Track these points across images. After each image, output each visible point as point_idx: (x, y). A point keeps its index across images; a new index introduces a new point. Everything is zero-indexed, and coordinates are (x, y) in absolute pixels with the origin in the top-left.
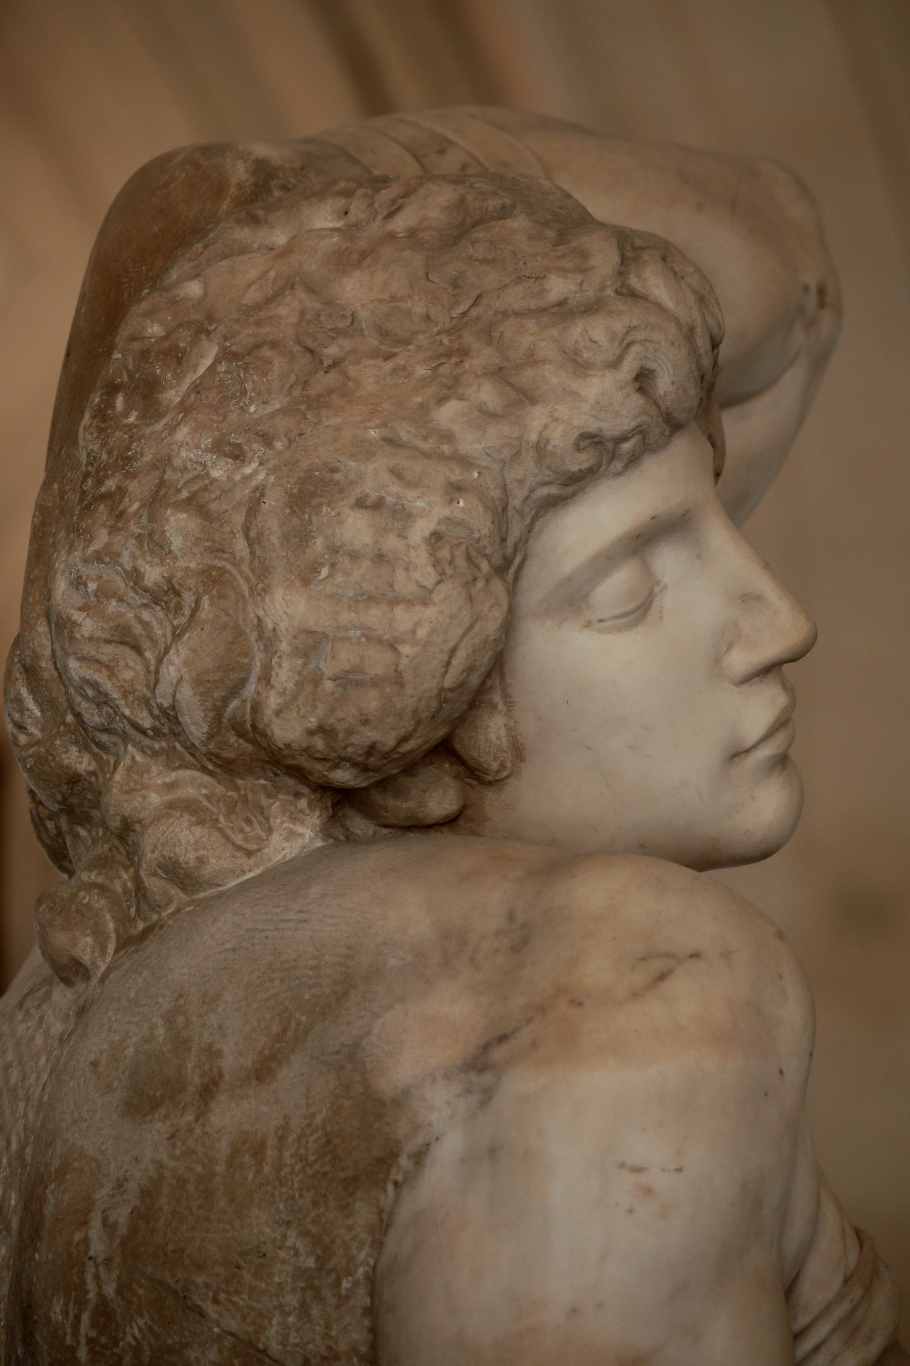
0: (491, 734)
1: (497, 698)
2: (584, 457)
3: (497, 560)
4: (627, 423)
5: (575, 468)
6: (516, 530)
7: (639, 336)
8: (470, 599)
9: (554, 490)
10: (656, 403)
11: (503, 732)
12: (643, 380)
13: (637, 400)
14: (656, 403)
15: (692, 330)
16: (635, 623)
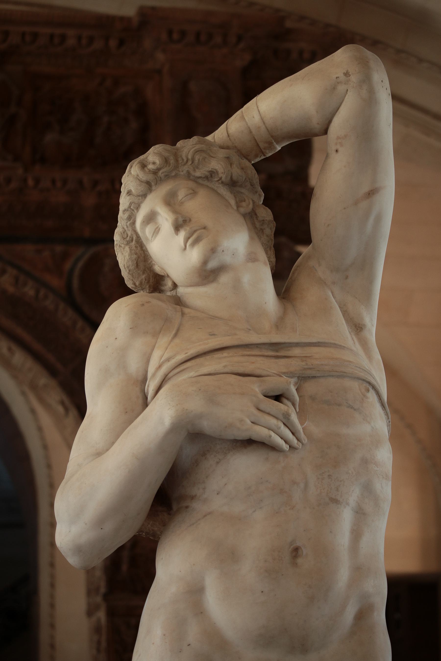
0: (157, 269)
1: (153, 263)
2: (126, 215)
3: (125, 243)
4: (128, 204)
5: (126, 218)
6: (129, 234)
7: (126, 184)
8: (123, 254)
9: (129, 223)
10: (134, 195)
11: (158, 268)
12: (129, 193)
13: (128, 198)
14: (134, 195)
15: (138, 175)
16: (156, 236)
